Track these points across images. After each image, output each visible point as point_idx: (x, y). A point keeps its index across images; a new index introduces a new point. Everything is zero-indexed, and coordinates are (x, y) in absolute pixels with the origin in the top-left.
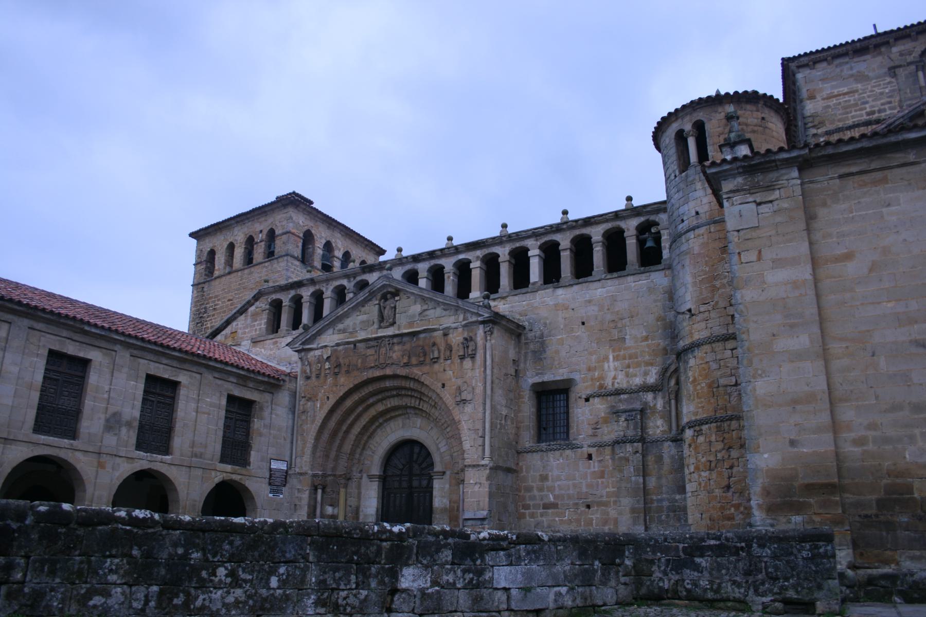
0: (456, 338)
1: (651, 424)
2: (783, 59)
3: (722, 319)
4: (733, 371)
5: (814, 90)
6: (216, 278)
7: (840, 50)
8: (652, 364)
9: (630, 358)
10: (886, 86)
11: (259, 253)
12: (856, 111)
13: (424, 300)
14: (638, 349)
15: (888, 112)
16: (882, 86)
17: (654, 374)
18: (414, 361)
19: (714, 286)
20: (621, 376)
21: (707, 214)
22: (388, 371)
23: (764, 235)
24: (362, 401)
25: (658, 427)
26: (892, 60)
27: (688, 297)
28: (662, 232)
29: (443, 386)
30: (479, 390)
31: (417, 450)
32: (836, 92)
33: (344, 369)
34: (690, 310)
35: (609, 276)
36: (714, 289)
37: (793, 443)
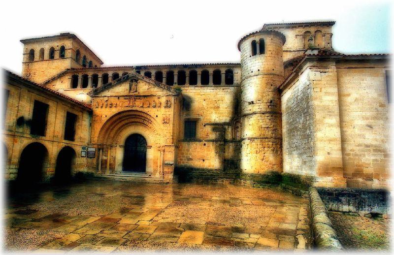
0: (163, 100)
6: (35, 62)
18: (145, 106)
19: (263, 95)
24: (120, 118)
29: (157, 116)
30: (172, 119)
34: (253, 102)
37: (329, 153)
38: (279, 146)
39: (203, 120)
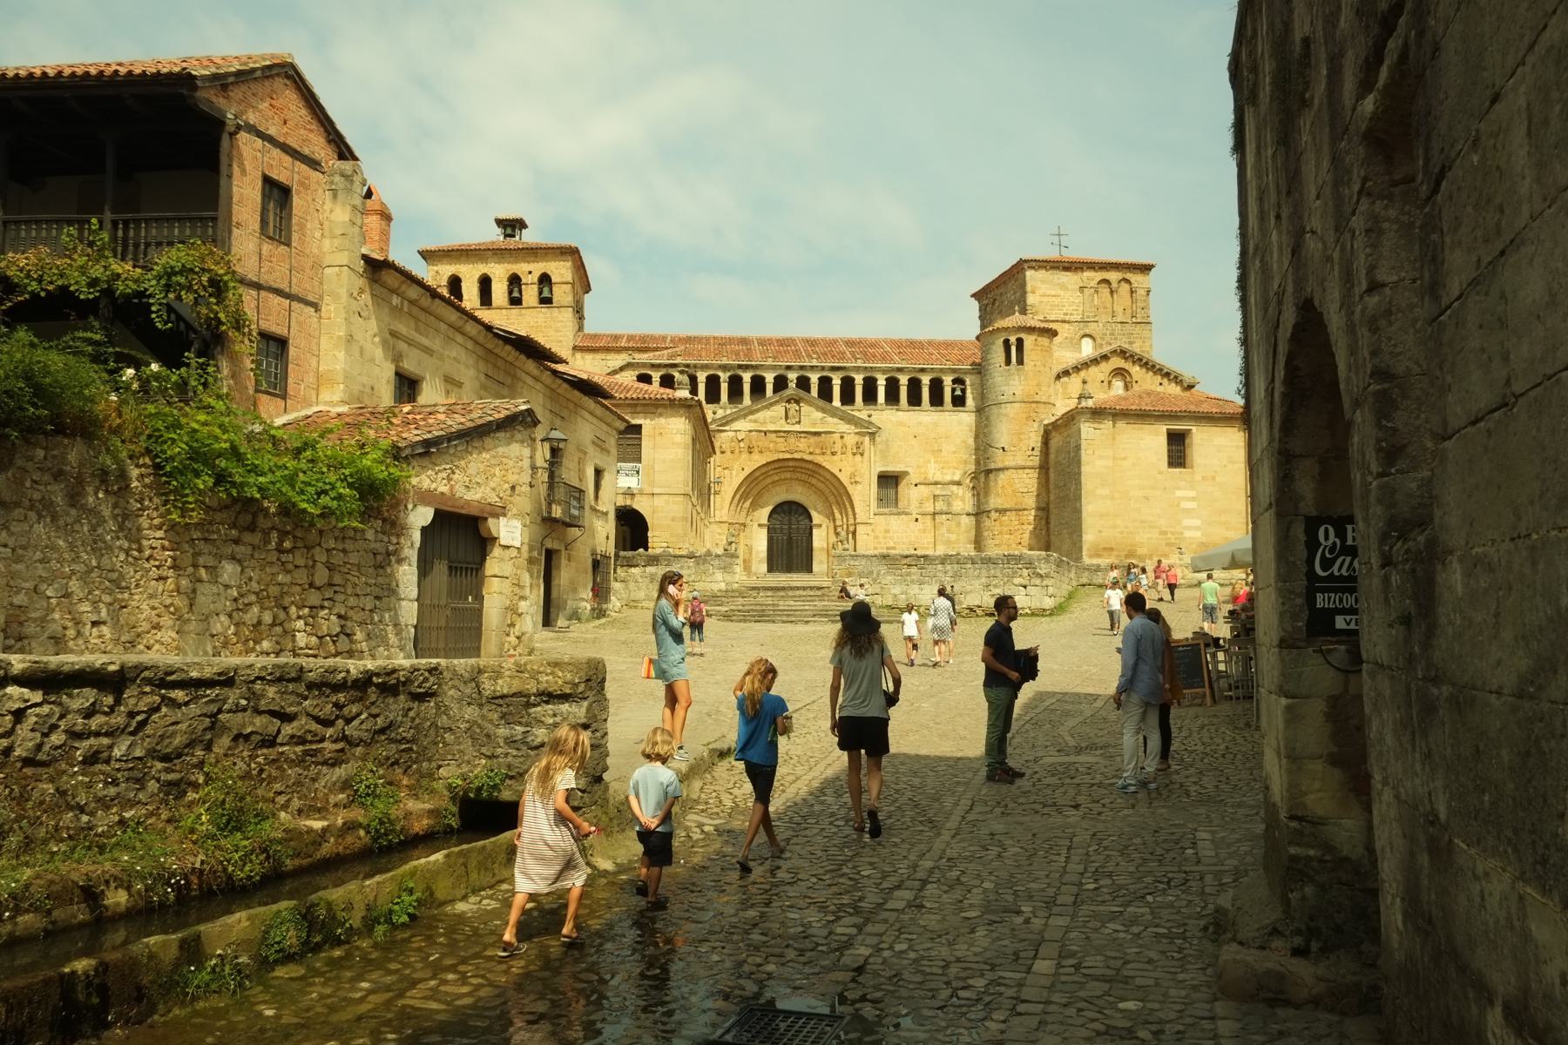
0: (851, 440)
10: (1077, 298)
11: (530, 294)
13: (823, 410)
20: (938, 474)
22: (796, 456)
27: (1003, 440)
31: (794, 507)
32: (1048, 292)
33: (756, 450)
35: (933, 408)
36: (1020, 440)
38: (1043, 522)
39: (914, 477)
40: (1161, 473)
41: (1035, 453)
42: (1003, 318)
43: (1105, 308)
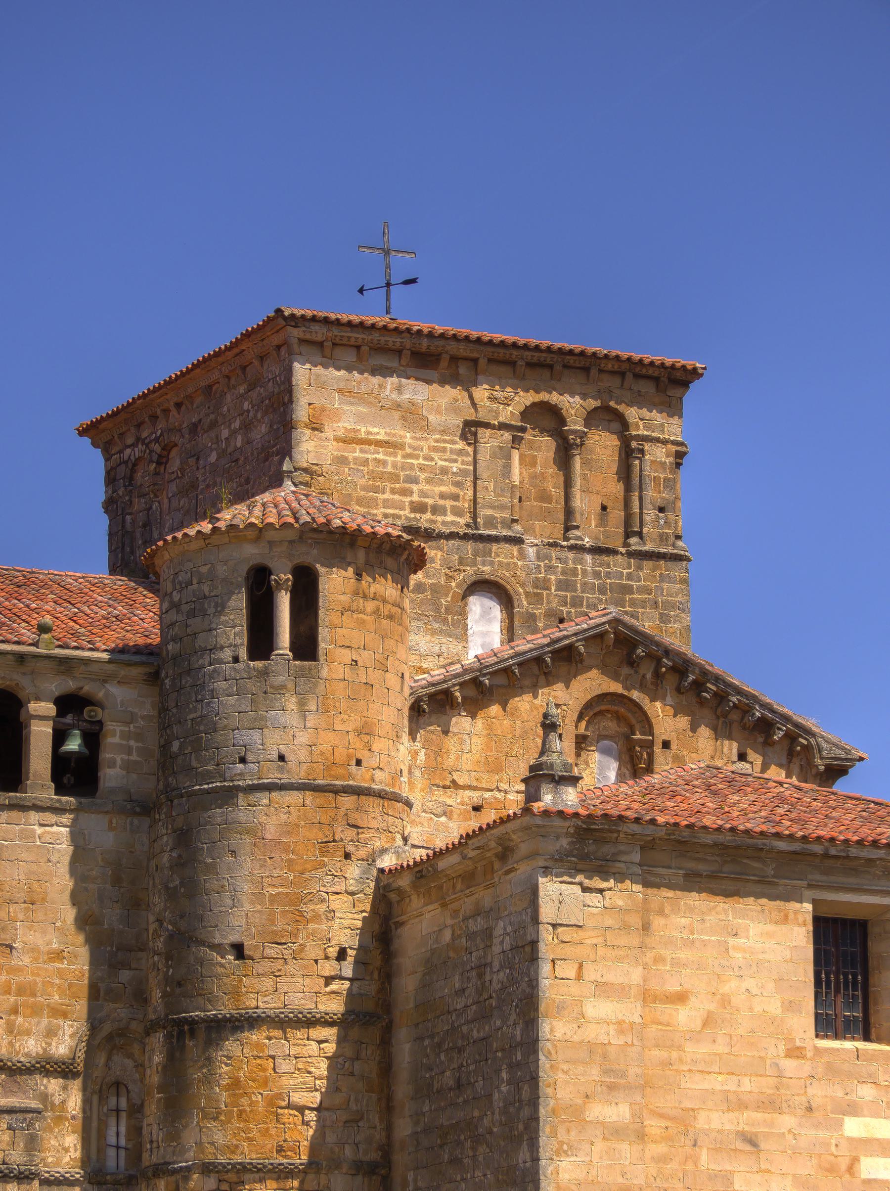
1: (53, 1142)
2: (279, 311)
3: (308, 981)
4: (318, 1082)
5: (323, 409)
7: (393, 341)
8: (65, 1015)
9: (20, 992)
12: (393, 491)
14: (38, 975)
15: (449, 518)
16: (448, 455)
17: (67, 1038)
21: (304, 767)
23: (588, 941)
25: (67, 1150)
26: (474, 405)
28: (109, 726)
40: (794, 1052)
41: (348, 969)
42: (242, 496)
43: (544, 497)
